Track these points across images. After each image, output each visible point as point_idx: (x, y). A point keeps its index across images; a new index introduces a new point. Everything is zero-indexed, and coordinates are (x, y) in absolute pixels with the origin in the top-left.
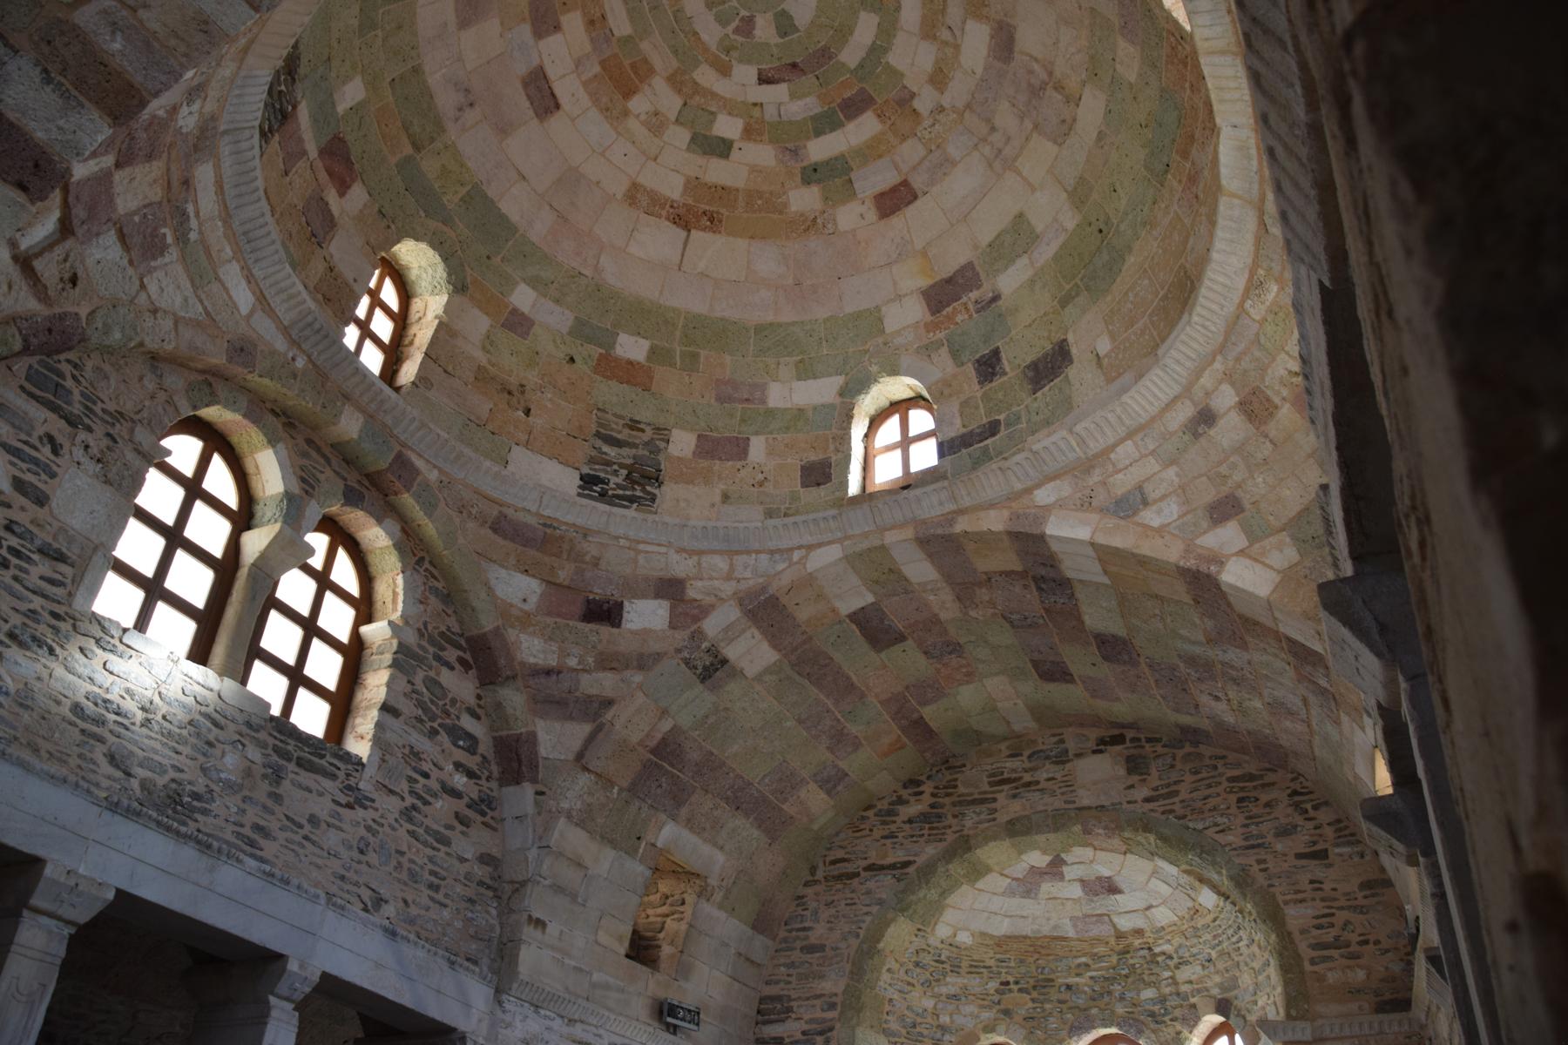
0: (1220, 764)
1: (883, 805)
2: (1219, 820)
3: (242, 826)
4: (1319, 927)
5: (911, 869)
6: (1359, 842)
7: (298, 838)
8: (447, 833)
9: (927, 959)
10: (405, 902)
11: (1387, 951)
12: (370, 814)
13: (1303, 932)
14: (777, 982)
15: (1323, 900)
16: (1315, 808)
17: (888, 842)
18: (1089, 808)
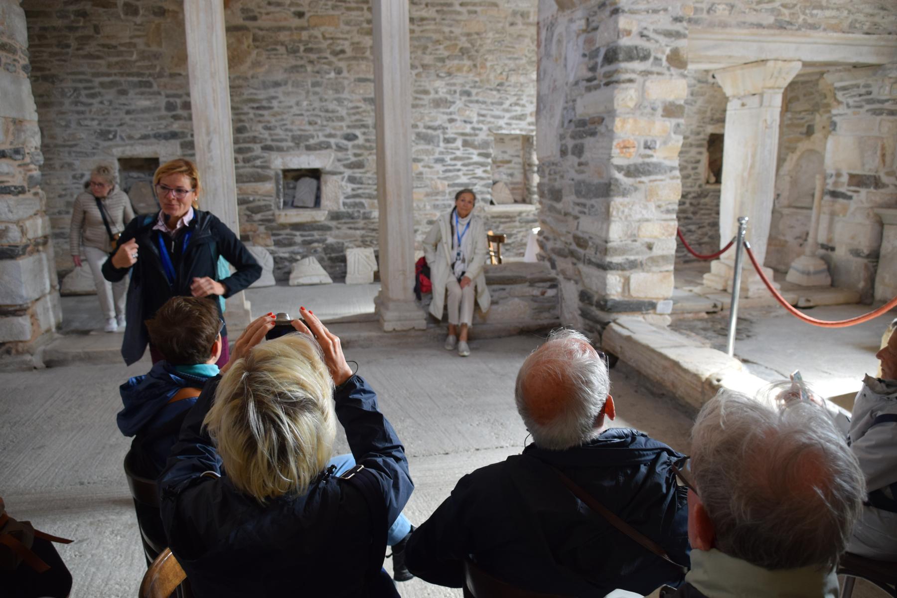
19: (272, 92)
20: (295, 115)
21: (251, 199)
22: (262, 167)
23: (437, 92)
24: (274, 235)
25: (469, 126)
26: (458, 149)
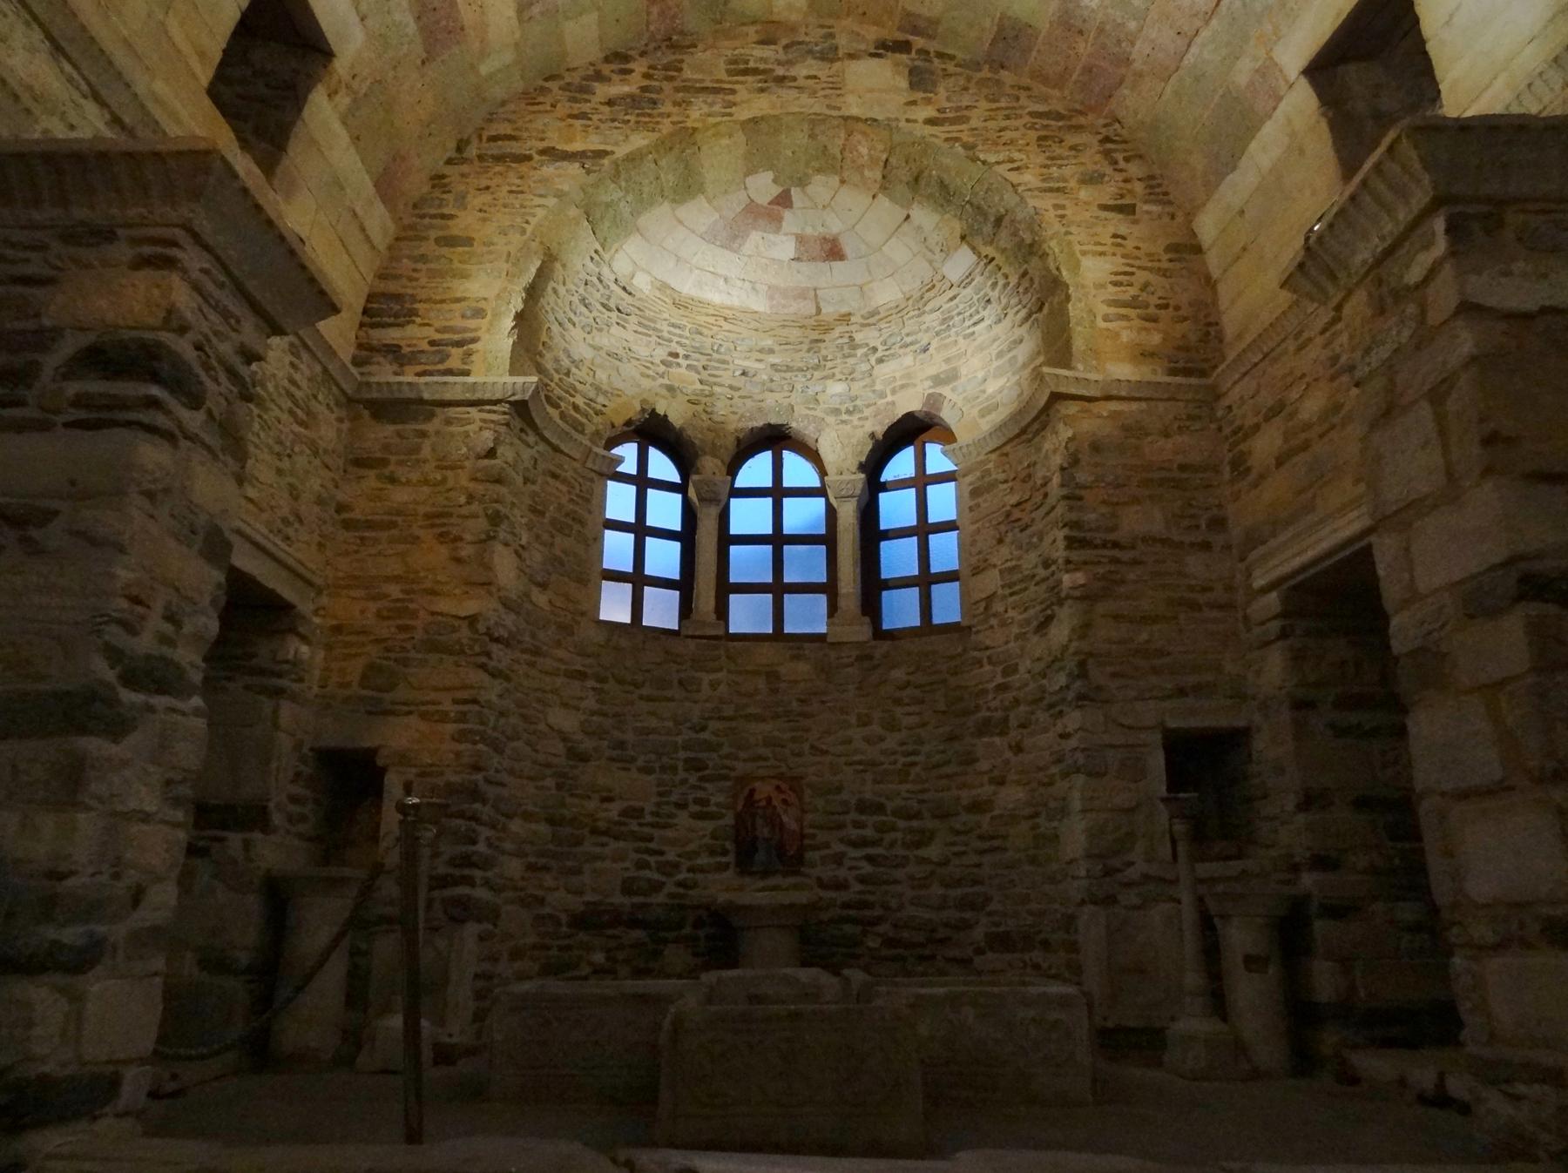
0: (1023, 94)
1: (575, 78)
2: (1016, 155)
4: (1115, 284)
5: (606, 161)
6: (1170, 203)
9: (595, 297)
11: (1185, 319)
13: (1101, 286)
14: (397, 277)
15: (1124, 256)
16: (1127, 160)
17: (578, 123)
18: (857, 119)
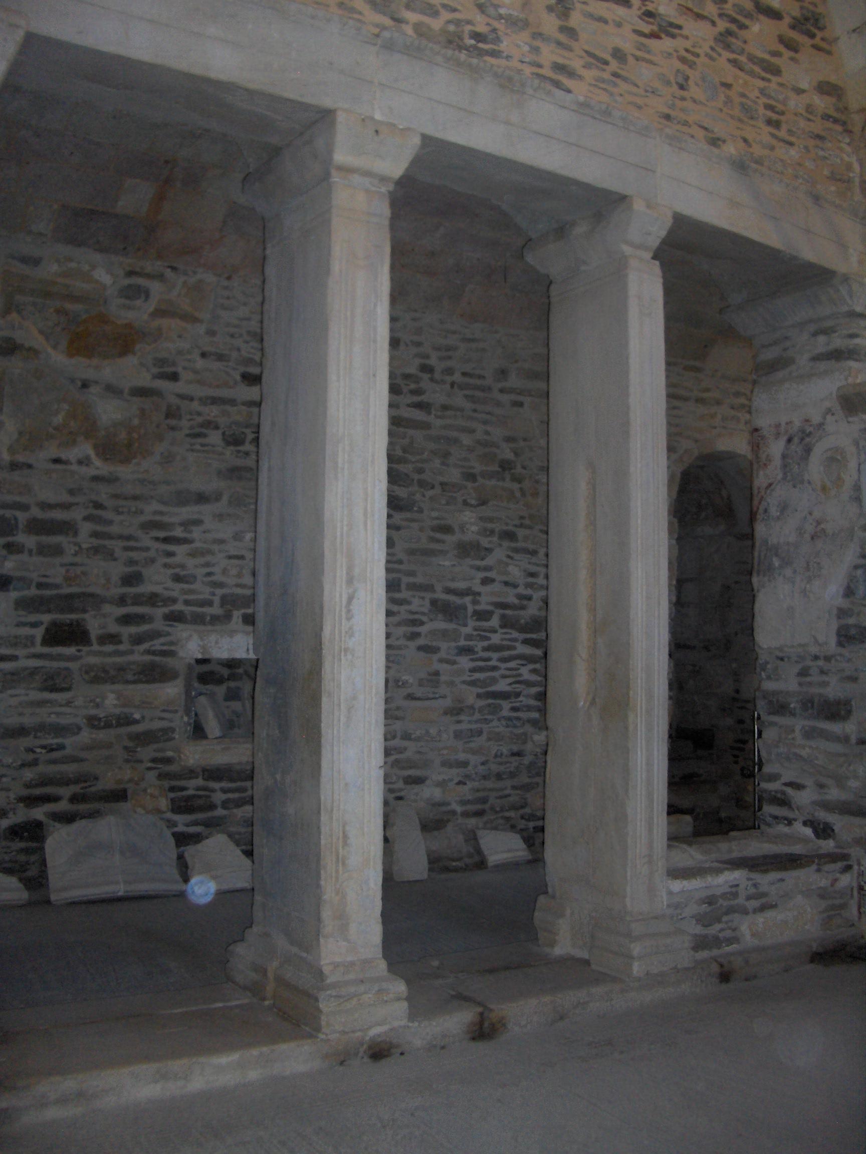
3: (540, 66)
7: (606, 76)
8: (774, 60)
10: (745, 140)
12: (679, 43)
19: (187, 512)
20: (230, 557)
21: (137, 716)
22: (164, 653)
23: (463, 532)
24: (172, 789)
25: (512, 592)
26: (495, 632)
